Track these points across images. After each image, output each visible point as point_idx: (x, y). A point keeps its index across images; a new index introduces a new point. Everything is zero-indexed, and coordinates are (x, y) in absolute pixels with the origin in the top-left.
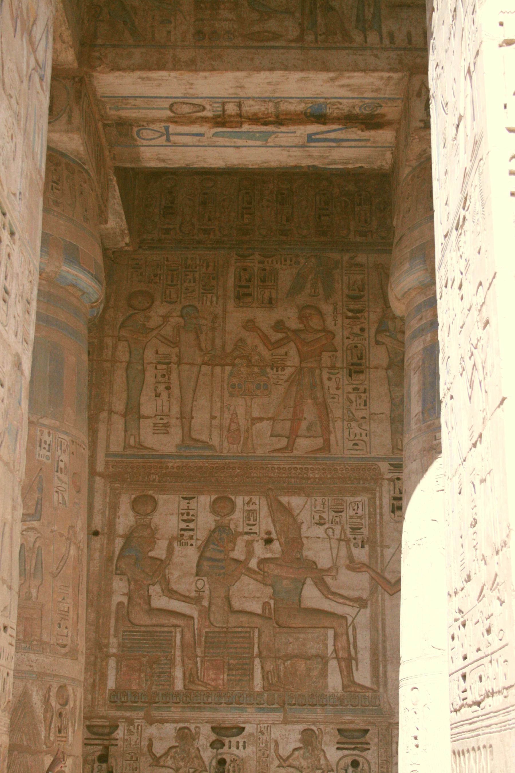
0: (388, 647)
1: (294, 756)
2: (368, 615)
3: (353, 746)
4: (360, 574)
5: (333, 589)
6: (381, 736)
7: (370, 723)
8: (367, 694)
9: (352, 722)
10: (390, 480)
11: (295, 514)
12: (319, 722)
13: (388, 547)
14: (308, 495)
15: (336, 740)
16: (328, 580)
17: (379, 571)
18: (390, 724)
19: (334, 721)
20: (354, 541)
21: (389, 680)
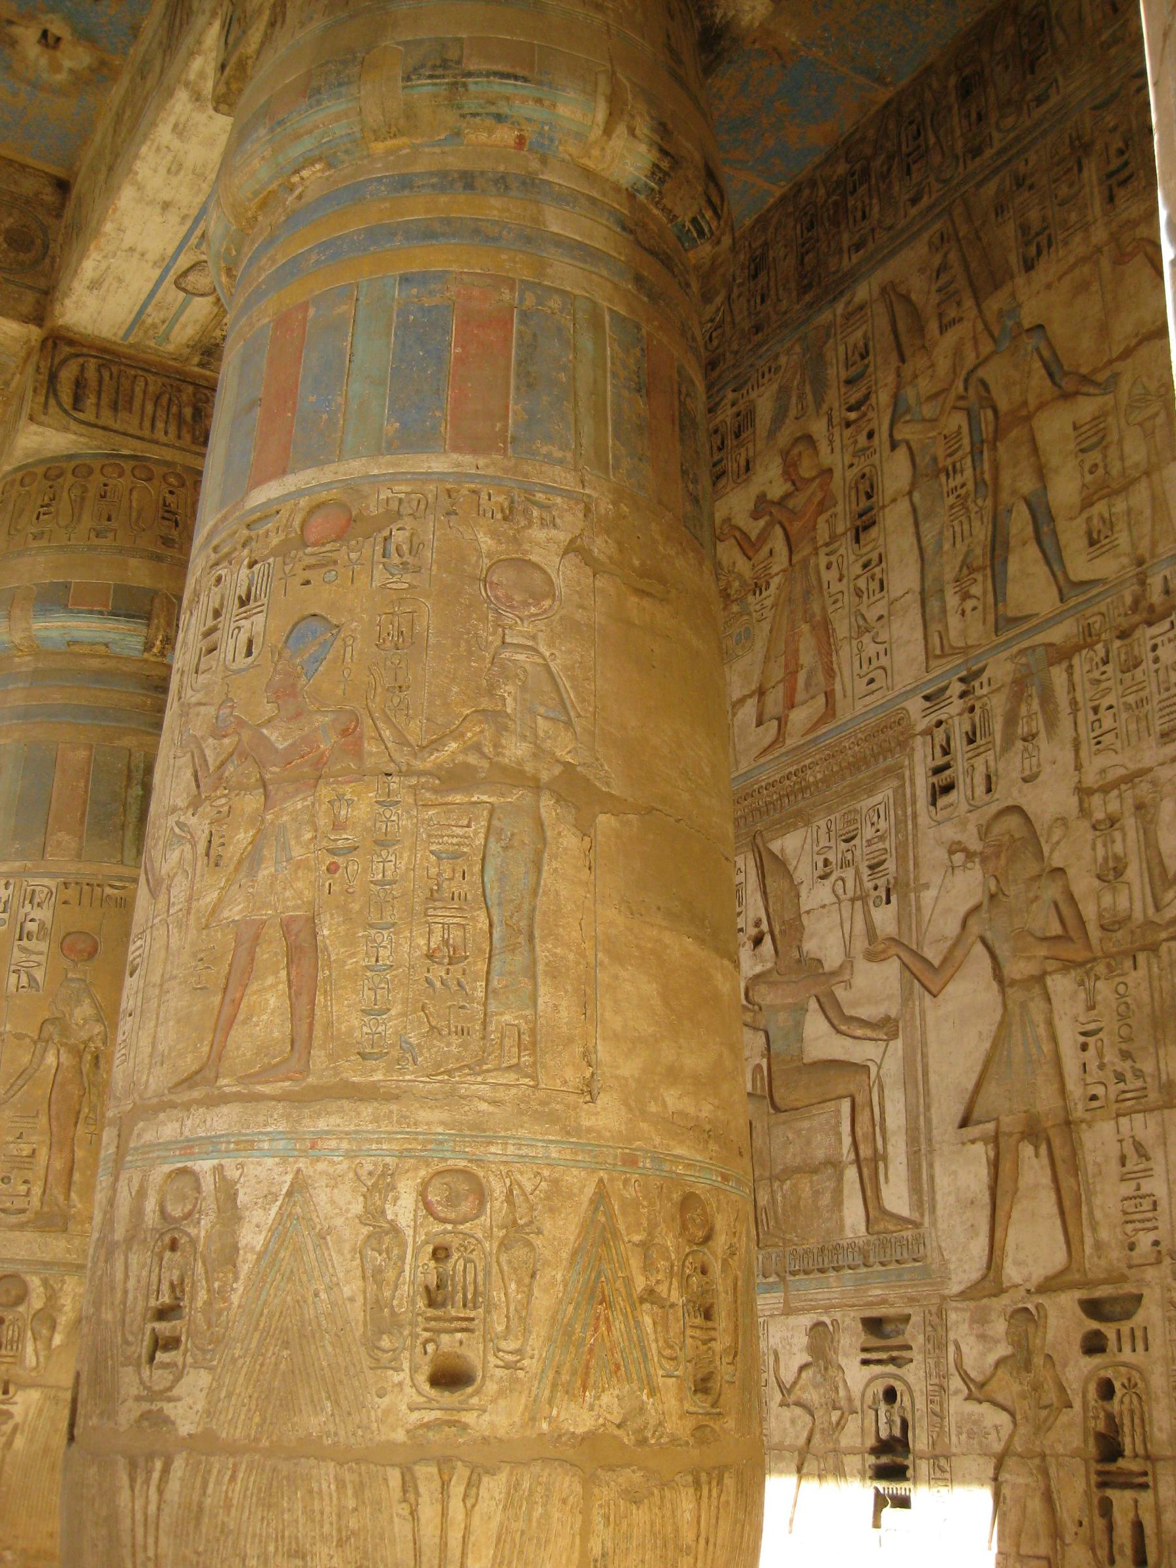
0: (935, 1121)
1: (801, 1382)
2: (900, 1053)
3: (884, 1356)
4: (884, 964)
5: (848, 1012)
6: (929, 1329)
7: (912, 1300)
8: (904, 1234)
9: (884, 1302)
10: (923, 733)
11: (791, 868)
12: (833, 1307)
13: (927, 886)
14: (808, 823)
15: (859, 1346)
16: (840, 993)
17: (914, 947)
18: (944, 1298)
19: (854, 1301)
20: (874, 894)
21: (939, 1197)
